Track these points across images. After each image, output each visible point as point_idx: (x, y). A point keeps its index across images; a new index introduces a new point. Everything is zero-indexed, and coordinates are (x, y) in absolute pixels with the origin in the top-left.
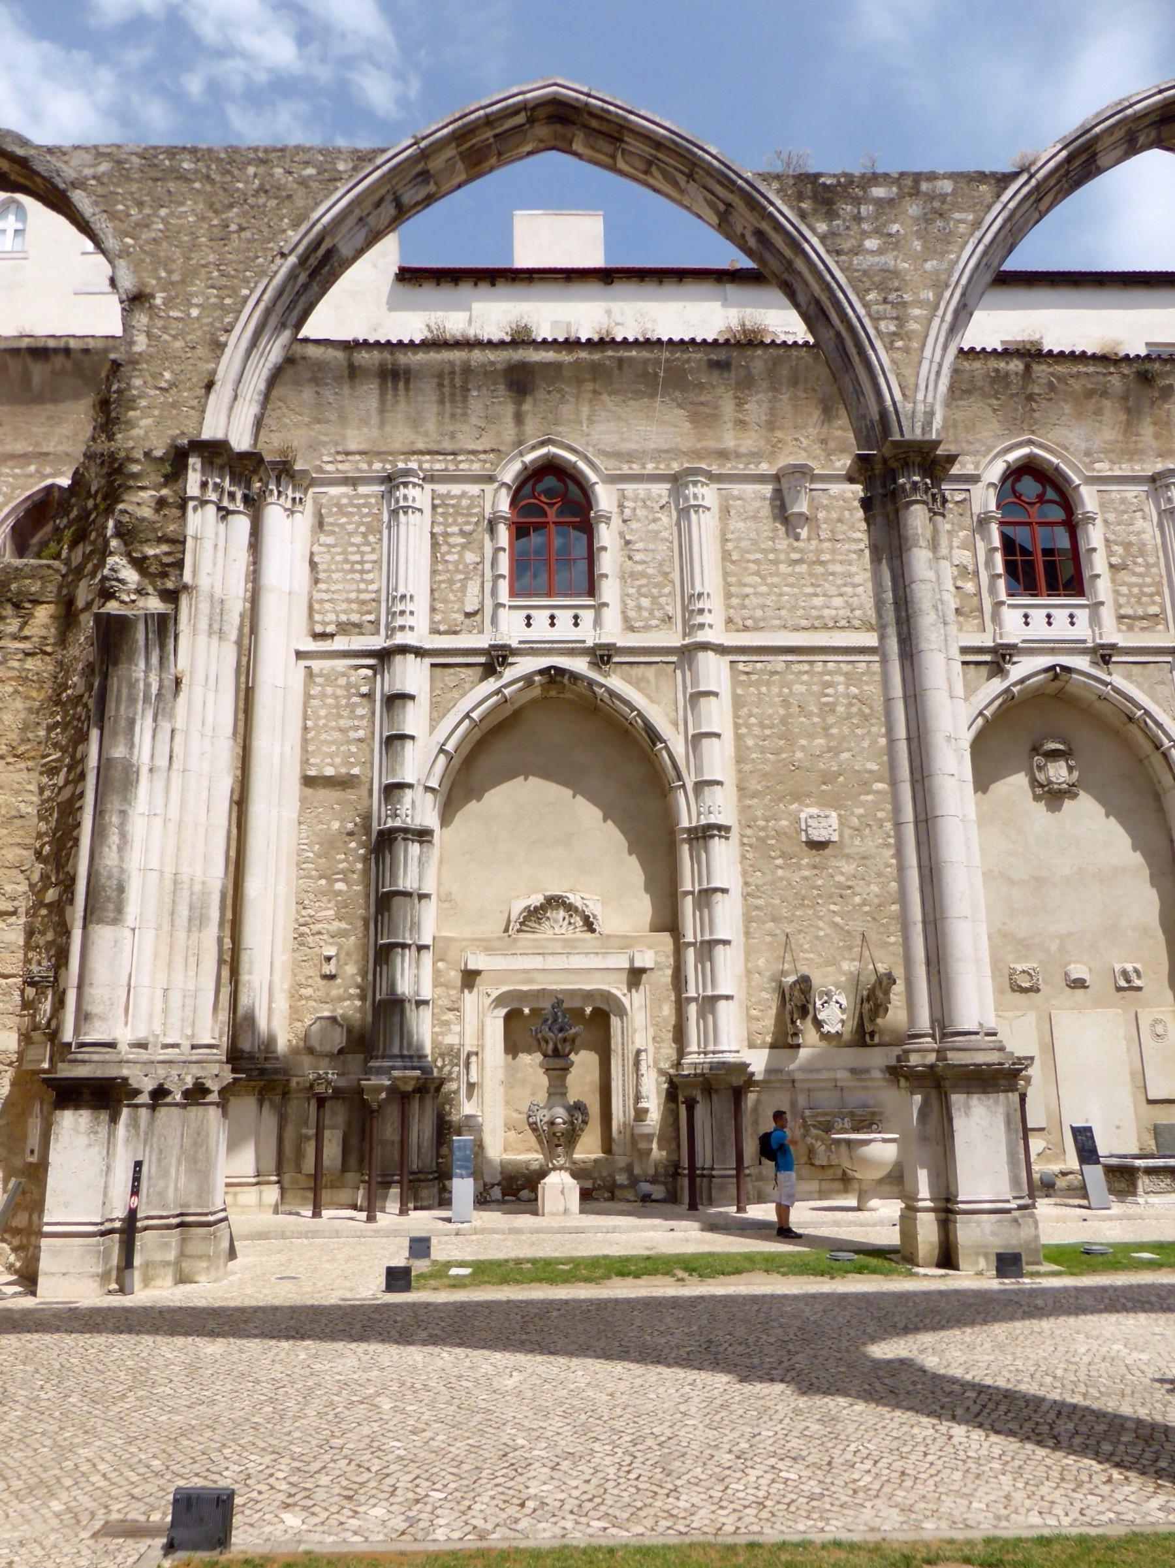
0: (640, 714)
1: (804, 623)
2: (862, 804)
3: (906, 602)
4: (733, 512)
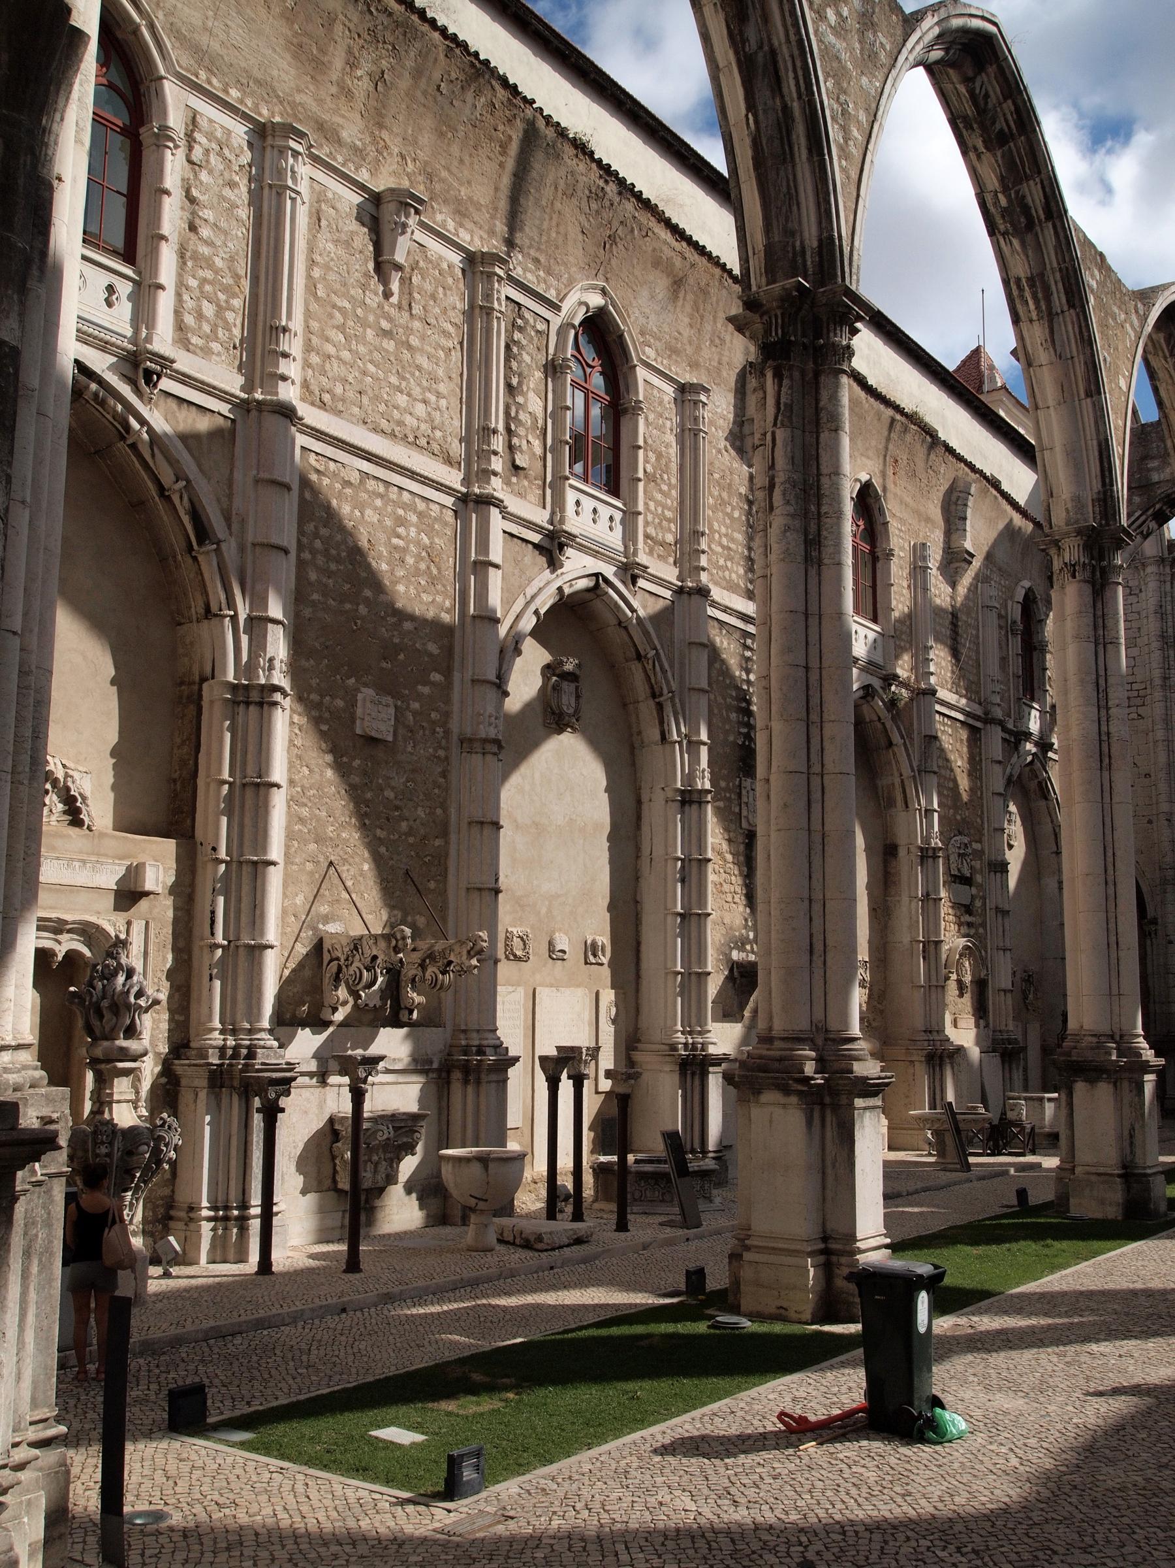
1: (384, 424)
2: (419, 697)
3: (819, 497)
4: (324, 223)
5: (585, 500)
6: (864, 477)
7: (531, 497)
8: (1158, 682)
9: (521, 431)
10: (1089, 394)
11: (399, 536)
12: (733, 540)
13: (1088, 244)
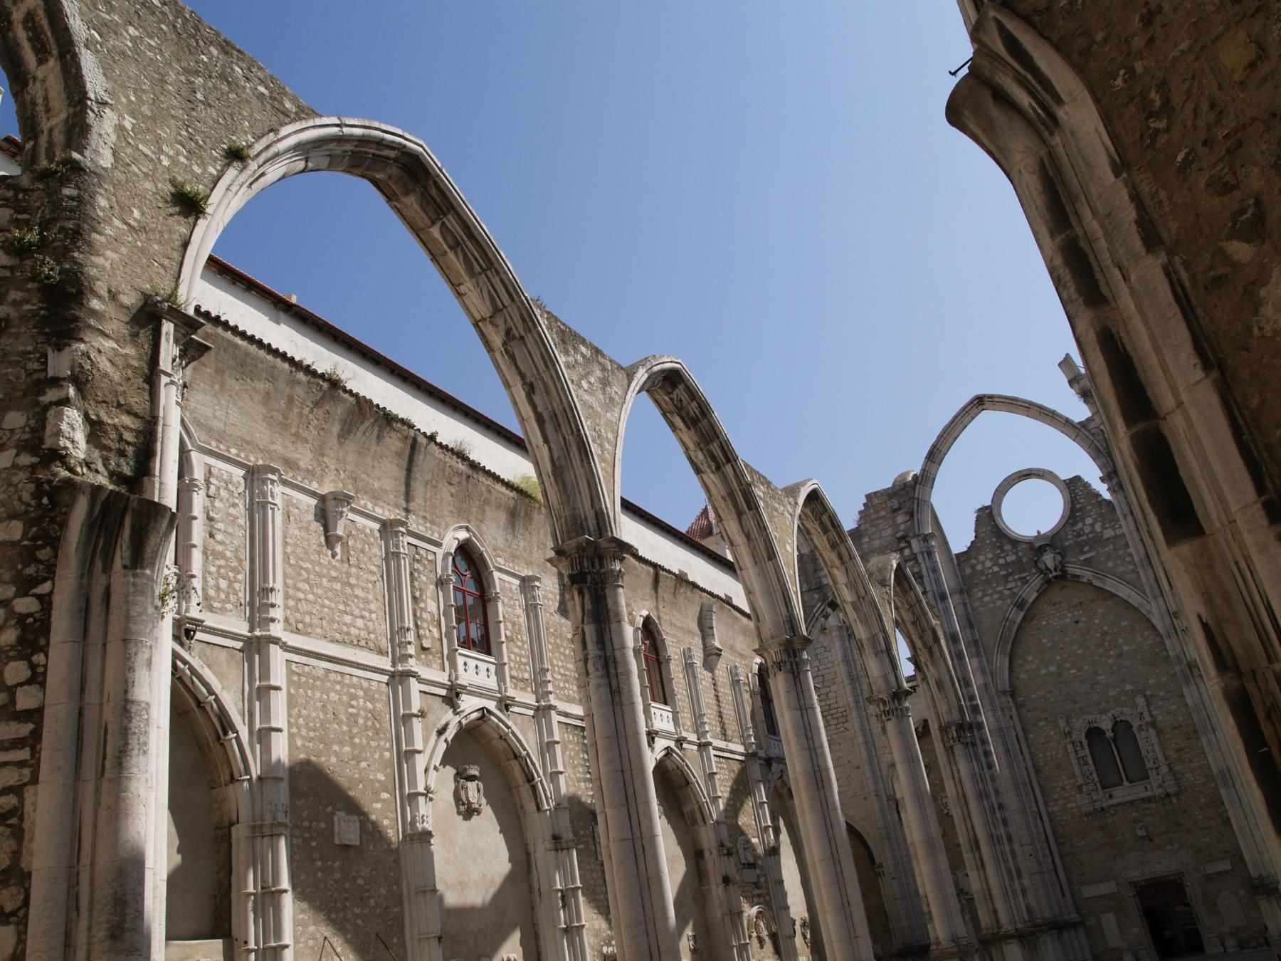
0: (217, 700)
1: (338, 636)
3: (615, 663)
5: (469, 661)
6: (645, 613)
7: (435, 666)
8: (852, 705)
9: (425, 625)
10: (770, 559)
11: (352, 707)
12: (567, 669)
13: (752, 471)
